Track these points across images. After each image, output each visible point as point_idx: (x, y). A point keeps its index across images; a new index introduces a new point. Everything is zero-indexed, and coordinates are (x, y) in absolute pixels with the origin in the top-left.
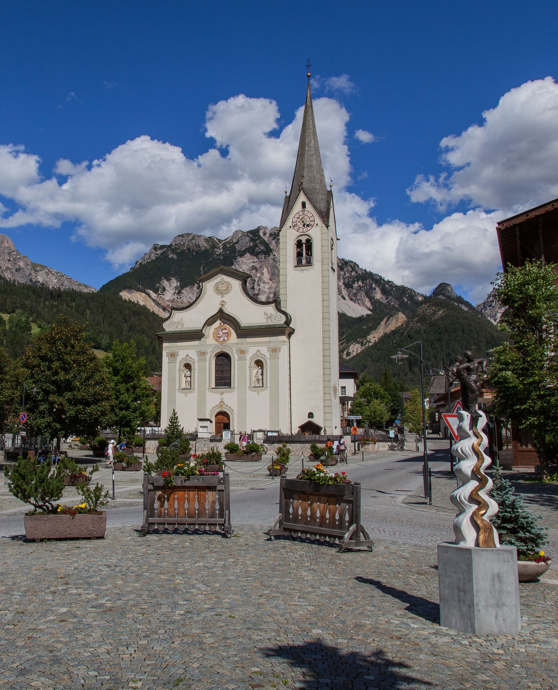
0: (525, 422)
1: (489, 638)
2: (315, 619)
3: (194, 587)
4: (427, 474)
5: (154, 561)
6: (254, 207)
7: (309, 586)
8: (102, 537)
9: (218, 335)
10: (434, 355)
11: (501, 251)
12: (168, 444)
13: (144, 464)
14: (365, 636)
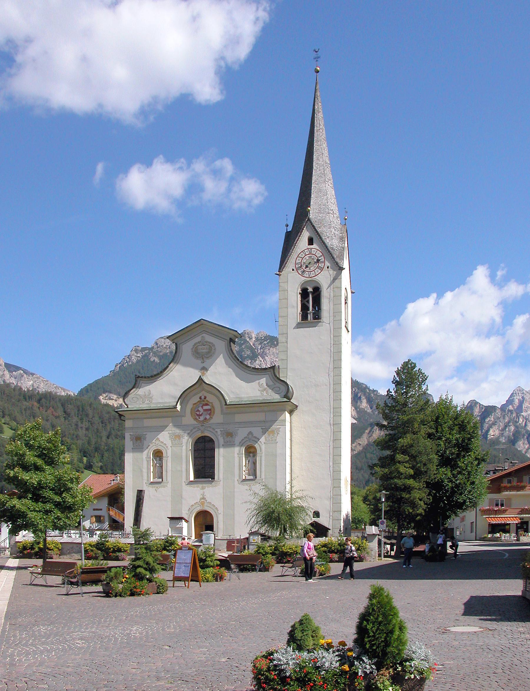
9: (198, 413)
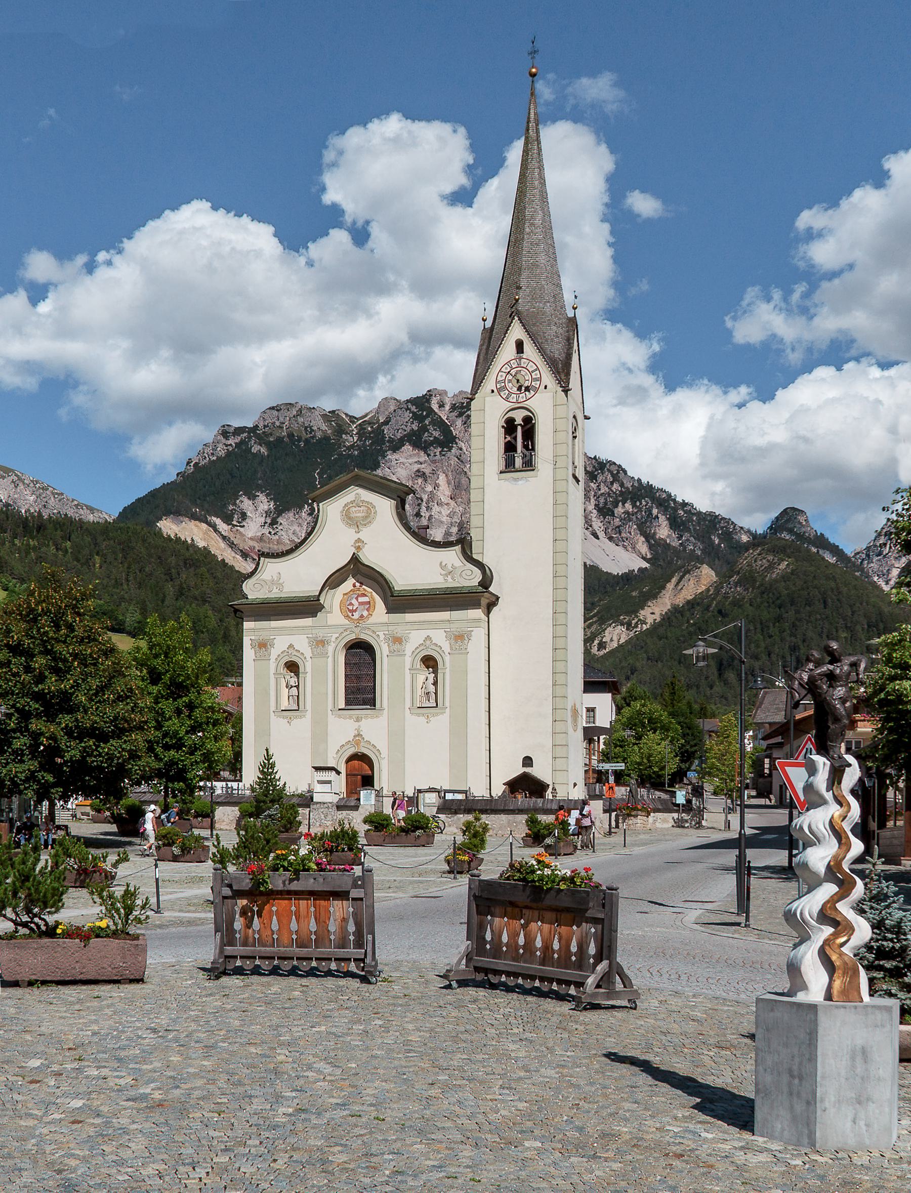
1: (839, 1156)
2: (529, 1124)
3: (310, 1068)
4: (743, 870)
5: (237, 1023)
6: (420, 350)
8: (140, 981)
9: (350, 608)
10: (766, 648)
12: (256, 814)
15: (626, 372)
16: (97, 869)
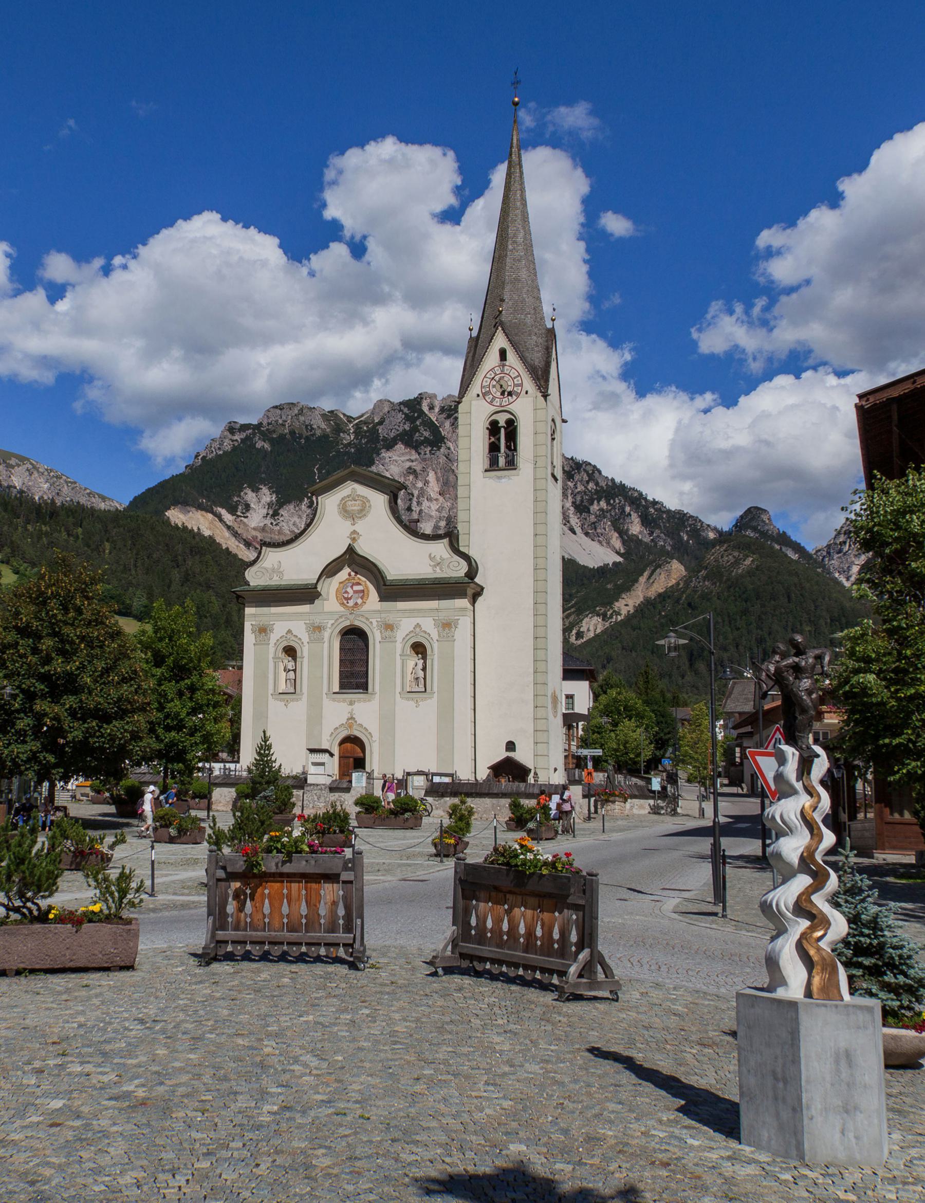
0: (899, 770)
1: (830, 1171)
2: (514, 1125)
3: (296, 1060)
4: (718, 859)
5: (226, 1012)
6: (412, 356)
7: (504, 1063)
8: (130, 967)
9: (346, 595)
10: (734, 639)
11: (862, 449)
12: (252, 795)
13: (209, 831)
14: (605, 1159)
15: (600, 380)
16: (94, 852)
